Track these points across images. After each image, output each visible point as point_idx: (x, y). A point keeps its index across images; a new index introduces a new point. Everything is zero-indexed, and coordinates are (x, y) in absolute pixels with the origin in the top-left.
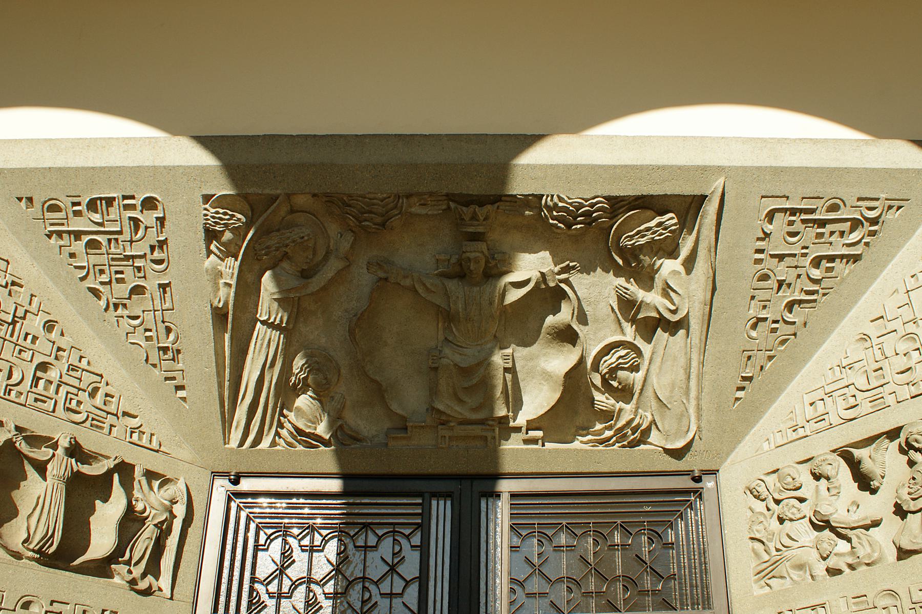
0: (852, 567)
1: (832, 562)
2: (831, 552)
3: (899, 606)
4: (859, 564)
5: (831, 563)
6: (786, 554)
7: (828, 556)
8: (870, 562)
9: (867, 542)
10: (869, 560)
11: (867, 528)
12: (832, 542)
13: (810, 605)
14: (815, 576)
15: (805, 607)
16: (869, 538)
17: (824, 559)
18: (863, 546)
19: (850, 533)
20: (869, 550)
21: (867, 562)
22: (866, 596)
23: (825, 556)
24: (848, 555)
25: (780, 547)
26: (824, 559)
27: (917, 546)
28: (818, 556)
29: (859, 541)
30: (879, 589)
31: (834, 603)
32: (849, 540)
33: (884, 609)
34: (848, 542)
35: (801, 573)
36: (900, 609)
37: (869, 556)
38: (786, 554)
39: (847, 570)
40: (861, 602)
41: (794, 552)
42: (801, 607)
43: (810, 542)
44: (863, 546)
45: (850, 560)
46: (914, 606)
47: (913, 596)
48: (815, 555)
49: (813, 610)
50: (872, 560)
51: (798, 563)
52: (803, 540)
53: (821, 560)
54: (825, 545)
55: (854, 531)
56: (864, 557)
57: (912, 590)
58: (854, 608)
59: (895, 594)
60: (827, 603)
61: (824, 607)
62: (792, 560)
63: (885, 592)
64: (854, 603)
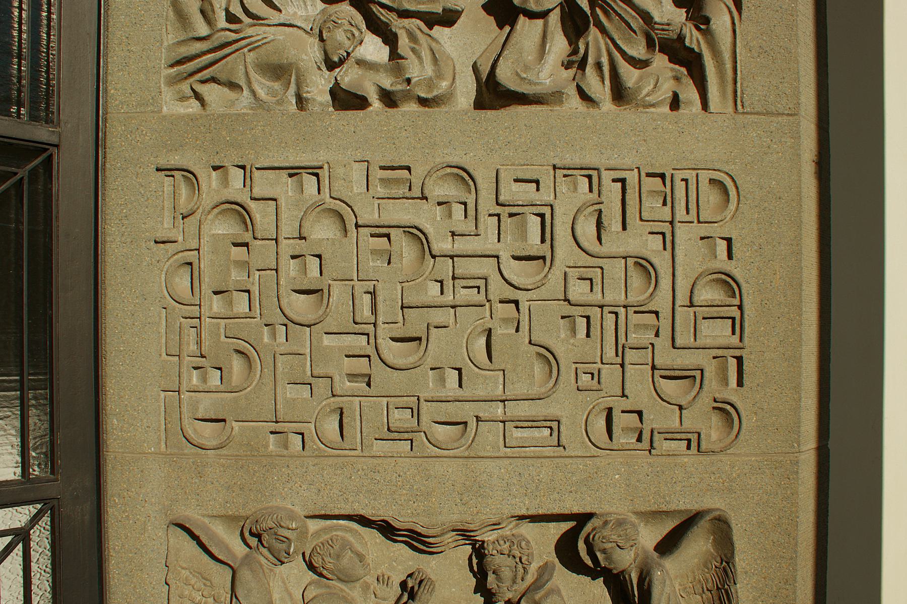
0: (389, 99)
1: (348, 77)
2: (348, 54)
4: (407, 96)
5: (347, 79)
6: (250, 31)
7: (342, 62)
8: (429, 96)
9: (428, 52)
10: (428, 92)
11: (431, 20)
12: (357, 33)
13: (287, 165)
14: (307, 100)
15: (276, 165)
16: (434, 45)
17: (331, 65)
18: (419, 58)
19: (398, 25)
20: (429, 71)
21: (423, 95)
22: (408, 169)
23: (336, 59)
24: (386, 71)
25: (237, 10)
26: (331, 65)
27: (528, 87)
28: (318, 56)
29: (413, 45)
30: (438, 160)
31: (340, 171)
32: (390, 39)
33: (439, 204)
34: (386, 42)
35: (277, 85)
36: (472, 212)
37: (430, 83)
38: (250, 31)
39: (376, 104)
40: (397, 181)
41: (271, 33)
42: (266, 165)
43: (306, 19)
44: (419, 58)
45: (387, 83)
46: (498, 209)
47: (502, 190)
48: (312, 53)
49: (291, 175)
50: (435, 93)
51: (275, 59)
52: (291, 10)
53: (324, 69)
54: (340, 36)
55: (406, 22)
56: (419, 83)
57: (502, 175)
58: (381, 191)
59: (467, 178)
60: (326, 166)
61: (317, 175)
62: (262, 51)
63: (449, 170)
64: (381, 180)
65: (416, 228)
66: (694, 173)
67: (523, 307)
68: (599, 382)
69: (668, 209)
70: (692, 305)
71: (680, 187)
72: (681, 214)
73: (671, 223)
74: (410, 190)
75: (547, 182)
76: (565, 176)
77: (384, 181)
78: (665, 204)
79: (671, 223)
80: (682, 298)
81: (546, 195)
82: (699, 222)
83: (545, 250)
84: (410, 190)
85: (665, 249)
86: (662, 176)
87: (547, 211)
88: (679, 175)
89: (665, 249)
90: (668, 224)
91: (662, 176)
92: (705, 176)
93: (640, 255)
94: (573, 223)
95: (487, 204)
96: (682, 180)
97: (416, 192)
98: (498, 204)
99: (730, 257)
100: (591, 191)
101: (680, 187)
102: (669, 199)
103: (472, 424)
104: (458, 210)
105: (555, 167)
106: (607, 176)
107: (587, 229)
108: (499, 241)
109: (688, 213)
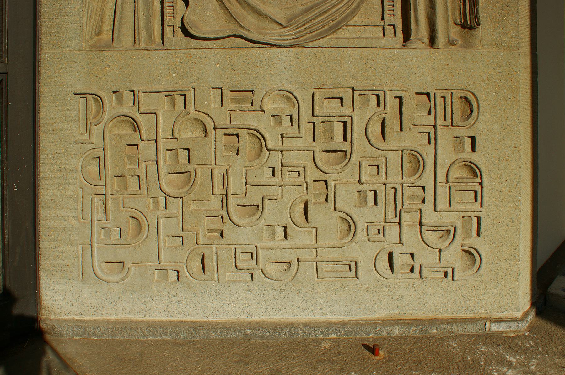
3: (295, 117)
58: (233, 106)
65: (257, 131)
66: (449, 92)
67: (331, 184)
68: (383, 236)
69: (432, 117)
70: (448, 182)
71: (440, 101)
72: (440, 122)
73: (435, 126)
74: (252, 105)
75: (348, 100)
76: (360, 95)
77: (235, 100)
78: (429, 113)
79: (435, 126)
80: (441, 178)
81: (347, 109)
82: (452, 125)
83: (346, 146)
84: (252, 105)
85: (429, 143)
86: (428, 95)
87: (348, 120)
88: (439, 95)
89: (429, 143)
90: (432, 127)
91: (428, 95)
92: (457, 94)
93: (413, 149)
94: (366, 128)
95: (306, 116)
96: (441, 97)
97: (257, 106)
98: (313, 115)
99: (473, 149)
100: (379, 105)
101: (440, 101)
102: (433, 109)
103: (295, 263)
104: (286, 121)
105: (353, 89)
106: (390, 96)
107: (376, 128)
108: (314, 140)
109: (445, 119)
